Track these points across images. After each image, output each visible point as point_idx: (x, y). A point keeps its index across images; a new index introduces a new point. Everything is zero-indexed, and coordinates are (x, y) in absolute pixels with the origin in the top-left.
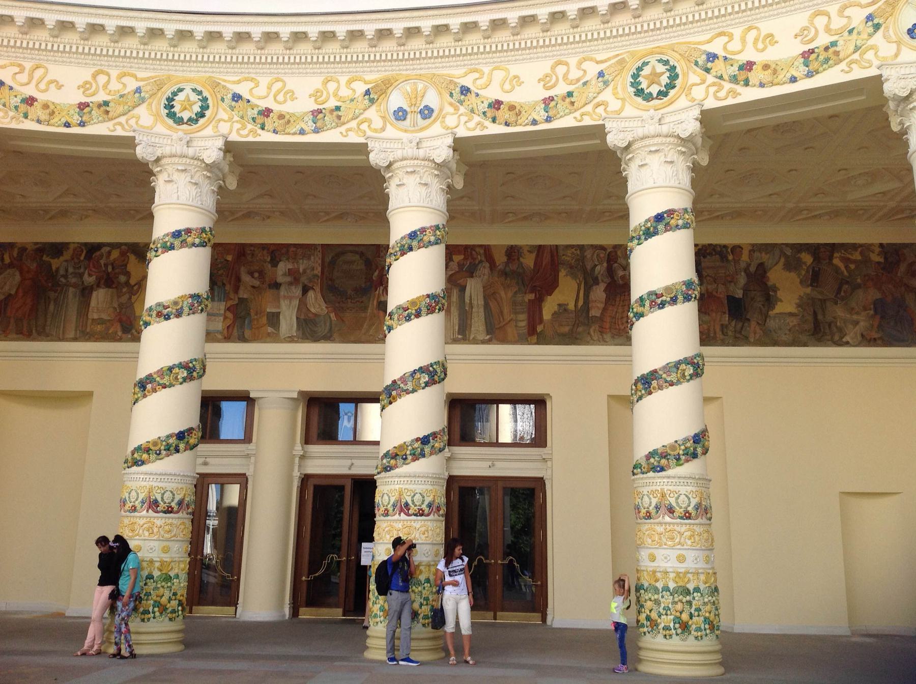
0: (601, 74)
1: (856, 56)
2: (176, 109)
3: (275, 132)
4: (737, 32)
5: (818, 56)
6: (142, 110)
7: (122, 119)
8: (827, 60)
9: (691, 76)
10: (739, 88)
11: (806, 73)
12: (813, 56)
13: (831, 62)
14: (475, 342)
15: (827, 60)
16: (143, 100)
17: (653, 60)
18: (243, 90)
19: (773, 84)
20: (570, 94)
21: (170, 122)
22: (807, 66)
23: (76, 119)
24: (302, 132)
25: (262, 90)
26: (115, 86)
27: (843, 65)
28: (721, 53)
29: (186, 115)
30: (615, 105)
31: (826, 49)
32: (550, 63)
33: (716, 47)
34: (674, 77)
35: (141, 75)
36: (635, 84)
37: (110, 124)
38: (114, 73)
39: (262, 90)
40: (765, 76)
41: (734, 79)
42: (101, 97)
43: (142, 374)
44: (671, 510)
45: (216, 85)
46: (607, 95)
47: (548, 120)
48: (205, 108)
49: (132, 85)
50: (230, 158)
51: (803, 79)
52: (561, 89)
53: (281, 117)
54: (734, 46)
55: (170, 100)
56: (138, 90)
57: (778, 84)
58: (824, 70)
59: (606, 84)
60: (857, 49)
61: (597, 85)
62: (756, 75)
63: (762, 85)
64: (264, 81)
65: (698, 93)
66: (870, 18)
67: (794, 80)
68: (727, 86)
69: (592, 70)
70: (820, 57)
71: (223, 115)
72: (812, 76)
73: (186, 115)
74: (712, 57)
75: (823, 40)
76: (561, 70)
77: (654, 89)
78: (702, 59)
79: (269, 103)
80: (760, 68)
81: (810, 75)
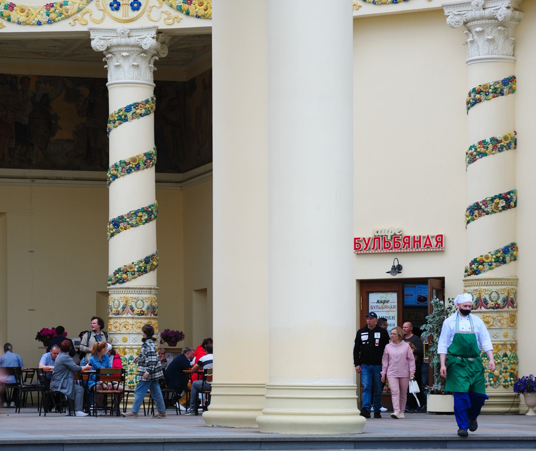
1: (79, 15)
5: (55, 10)
8: (61, 14)
10: (5, 23)
11: (47, 20)
12: (52, 9)
13: (63, 16)
15: (61, 14)
19: (25, 24)
22: (48, 16)
27: (70, 20)
31: (61, 6)
40: (23, 18)
51: (46, 24)
57: (29, 24)
58: (59, 20)
60: (79, 10)
62: (15, 15)
63: (19, 23)
67: (39, 23)
70: (57, 11)
72: (51, 23)
80: (19, 9)
81: (50, 22)
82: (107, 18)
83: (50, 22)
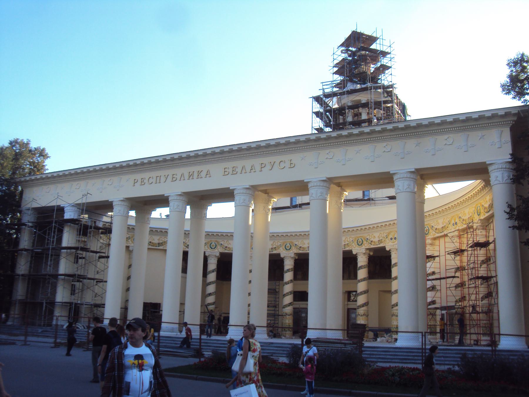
0: (352, 240)
2: (287, 247)
3: (302, 251)
4: (371, 235)
6: (281, 248)
7: (278, 250)
9: (365, 242)
10: (371, 245)
14: (352, 279)
16: (281, 246)
17: (360, 238)
18: (297, 243)
20: (348, 244)
21: (286, 250)
23: (271, 251)
24: (306, 251)
25: (300, 243)
26: (276, 244)
28: (369, 238)
29: (288, 249)
30: (354, 246)
32: (345, 238)
33: (368, 237)
34: (362, 242)
35: (280, 242)
36: (357, 243)
37: (276, 251)
38: (276, 242)
39: (300, 243)
41: (370, 244)
42: (275, 246)
43: (284, 294)
44: (359, 315)
45: (292, 243)
46: (353, 244)
47: (345, 248)
48: (291, 247)
49: (279, 244)
50: (296, 254)
52: (347, 243)
53: (303, 248)
54: (370, 237)
55: (285, 246)
56: (280, 245)
59: (353, 242)
60: (384, 241)
61: (352, 242)
62: (373, 243)
64: (300, 241)
65: (366, 245)
66: (386, 236)
67: (377, 245)
68: (369, 244)
69: (351, 239)
71: (294, 248)
73: (288, 249)
74: (367, 239)
75: (381, 238)
76: (347, 239)
77: (360, 244)
78: (366, 239)
79: (301, 245)
82: (390, 243)
83: (379, 244)
